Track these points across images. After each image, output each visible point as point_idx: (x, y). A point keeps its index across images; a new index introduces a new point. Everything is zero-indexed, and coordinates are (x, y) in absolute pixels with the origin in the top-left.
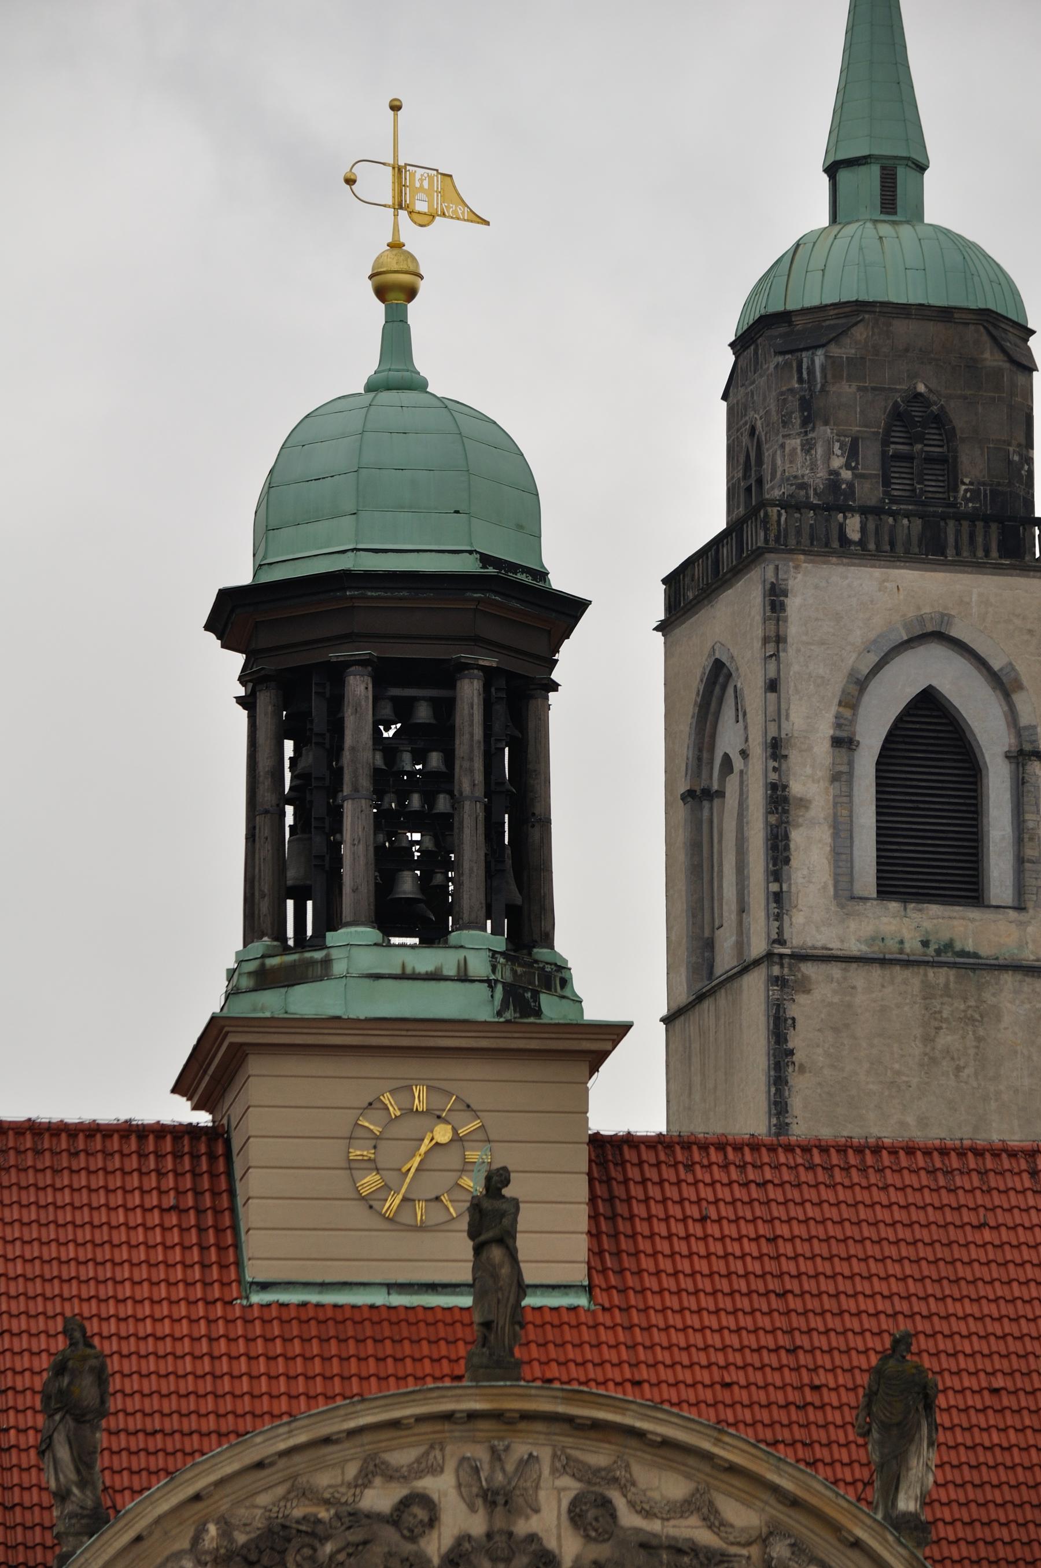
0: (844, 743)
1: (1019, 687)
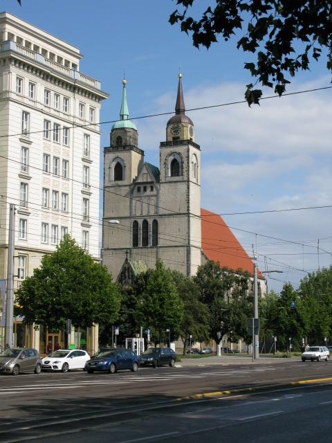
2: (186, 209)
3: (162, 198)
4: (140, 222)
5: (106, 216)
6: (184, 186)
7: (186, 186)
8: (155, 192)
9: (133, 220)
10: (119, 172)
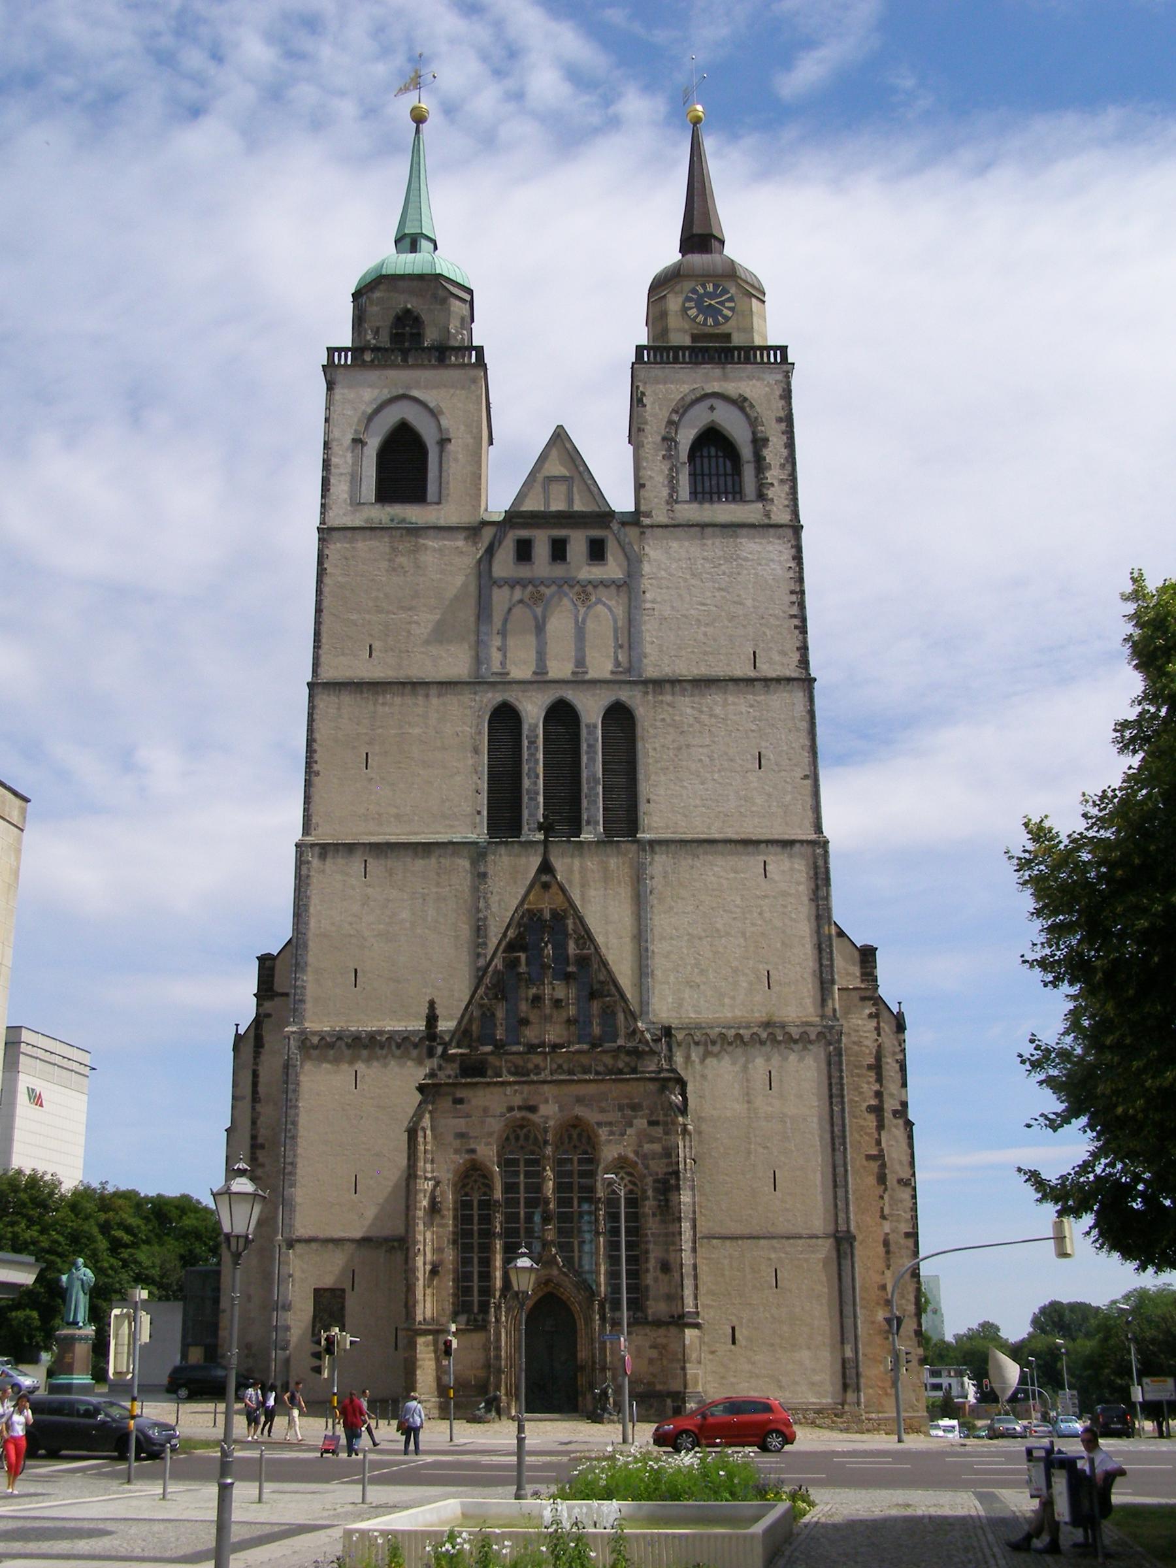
1: (442, 413)
2: (796, 656)
4: (533, 710)
5: (326, 675)
6: (776, 550)
7: (788, 553)
8: (612, 569)
9: (493, 698)
10: (403, 466)
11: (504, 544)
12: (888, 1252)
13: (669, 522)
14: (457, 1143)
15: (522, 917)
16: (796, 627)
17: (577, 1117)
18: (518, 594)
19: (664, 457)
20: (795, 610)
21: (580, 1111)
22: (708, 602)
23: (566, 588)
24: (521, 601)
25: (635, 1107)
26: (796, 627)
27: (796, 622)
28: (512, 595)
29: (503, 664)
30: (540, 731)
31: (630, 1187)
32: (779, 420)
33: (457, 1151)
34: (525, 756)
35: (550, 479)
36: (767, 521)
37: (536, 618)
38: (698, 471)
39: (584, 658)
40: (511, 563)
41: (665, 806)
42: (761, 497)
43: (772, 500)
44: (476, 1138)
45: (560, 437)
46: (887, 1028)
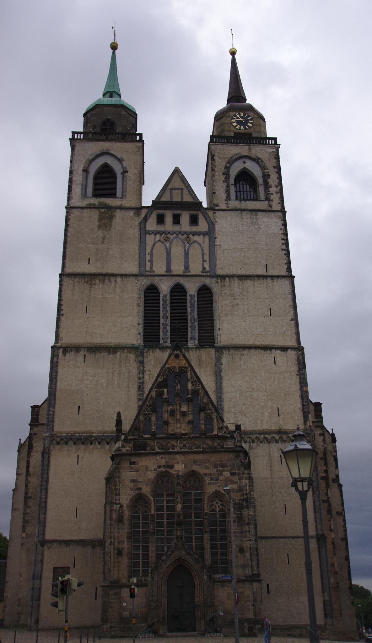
0: (86, 171)
2: (286, 267)
3: (220, 240)
4: (165, 287)
5: (68, 270)
7: (280, 223)
9: (146, 282)
11: (152, 215)
12: (334, 548)
13: (227, 208)
14: (131, 485)
15: (165, 371)
16: (285, 254)
17: (193, 471)
18: (158, 237)
19: (223, 181)
20: (284, 247)
21: (195, 468)
22: (245, 242)
23: (180, 236)
24: (159, 241)
25: (224, 466)
26: (285, 254)
27: (285, 252)
28: (155, 238)
29: (151, 267)
30: (168, 298)
31: (221, 507)
32: (274, 167)
33: (131, 489)
34: (161, 308)
35: (172, 189)
36: (270, 209)
37: (166, 248)
38: (238, 190)
39: (188, 267)
40: (155, 225)
41: (227, 330)
42: (268, 199)
43: (272, 200)
44: (142, 482)
45: (177, 171)
46: (329, 440)
